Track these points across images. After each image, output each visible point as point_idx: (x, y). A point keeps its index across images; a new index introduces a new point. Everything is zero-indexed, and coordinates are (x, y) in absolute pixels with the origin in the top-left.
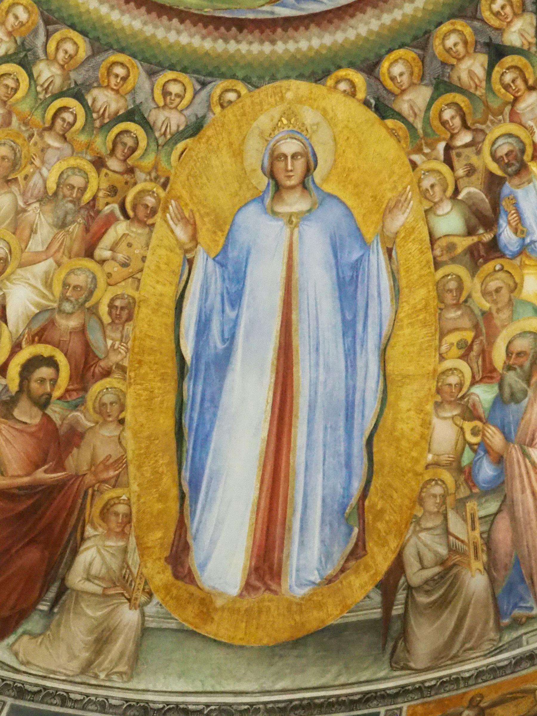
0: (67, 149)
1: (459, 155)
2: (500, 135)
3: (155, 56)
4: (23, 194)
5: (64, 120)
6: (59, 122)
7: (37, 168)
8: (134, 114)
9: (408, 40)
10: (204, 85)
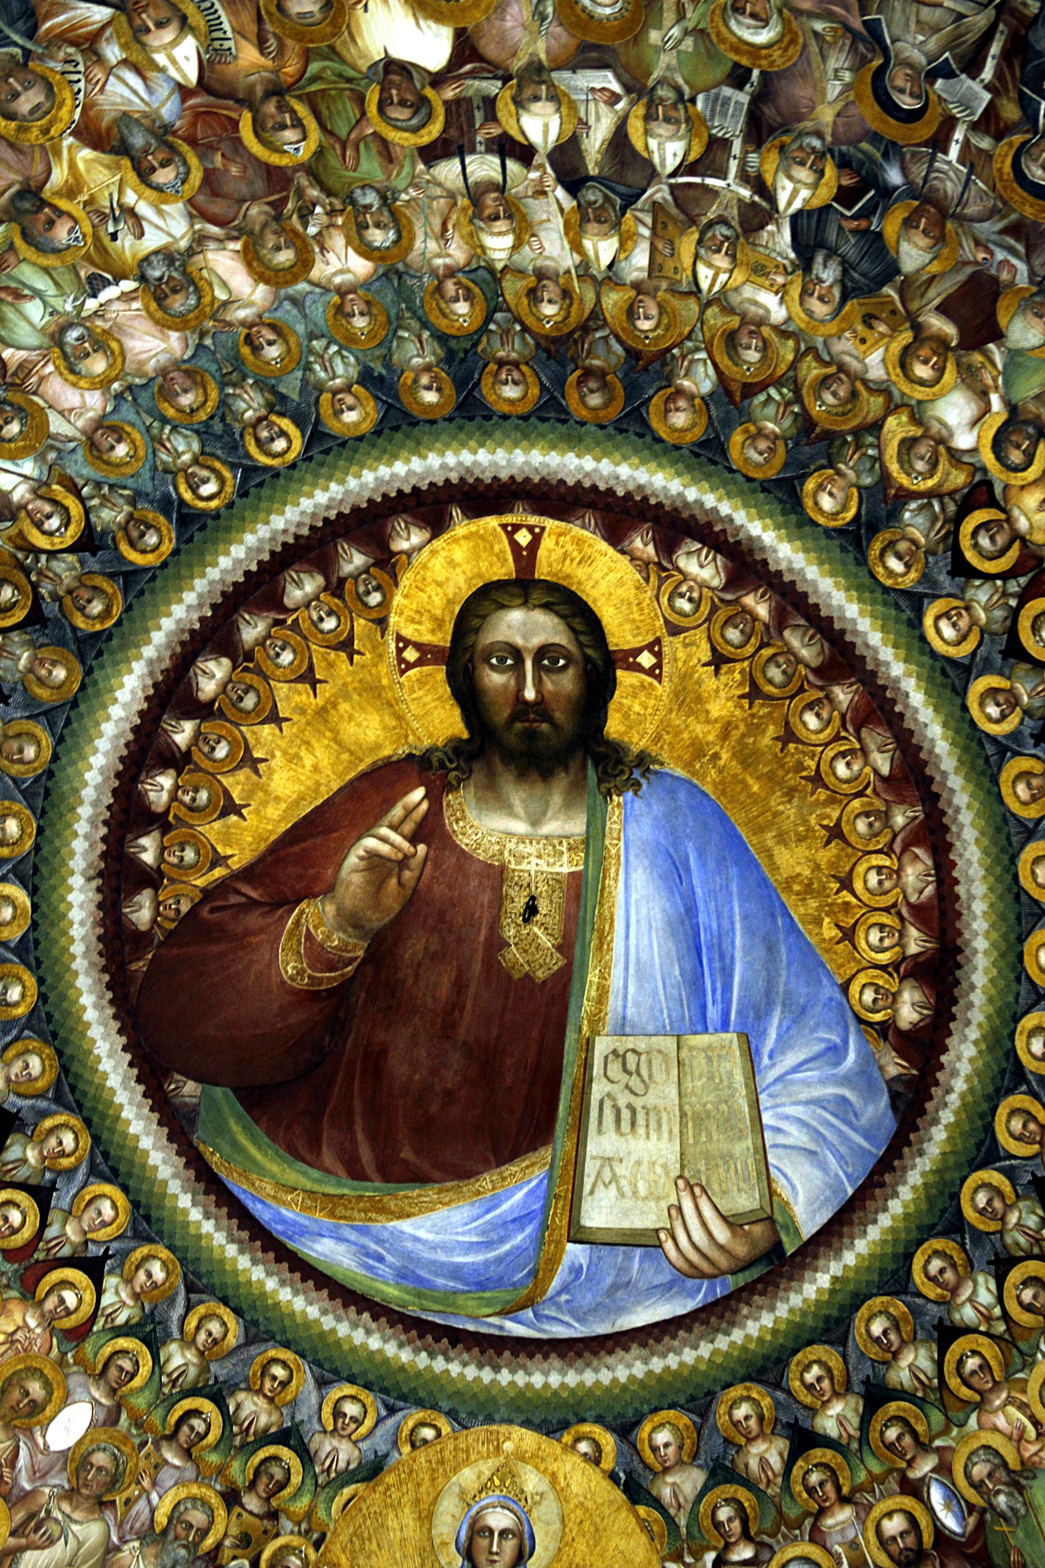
0: (190, 1473)
3: (330, 1359)
4: (120, 1526)
5: (192, 1428)
6: (185, 1429)
7: (144, 1490)
8: (289, 1436)
10: (392, 1410)
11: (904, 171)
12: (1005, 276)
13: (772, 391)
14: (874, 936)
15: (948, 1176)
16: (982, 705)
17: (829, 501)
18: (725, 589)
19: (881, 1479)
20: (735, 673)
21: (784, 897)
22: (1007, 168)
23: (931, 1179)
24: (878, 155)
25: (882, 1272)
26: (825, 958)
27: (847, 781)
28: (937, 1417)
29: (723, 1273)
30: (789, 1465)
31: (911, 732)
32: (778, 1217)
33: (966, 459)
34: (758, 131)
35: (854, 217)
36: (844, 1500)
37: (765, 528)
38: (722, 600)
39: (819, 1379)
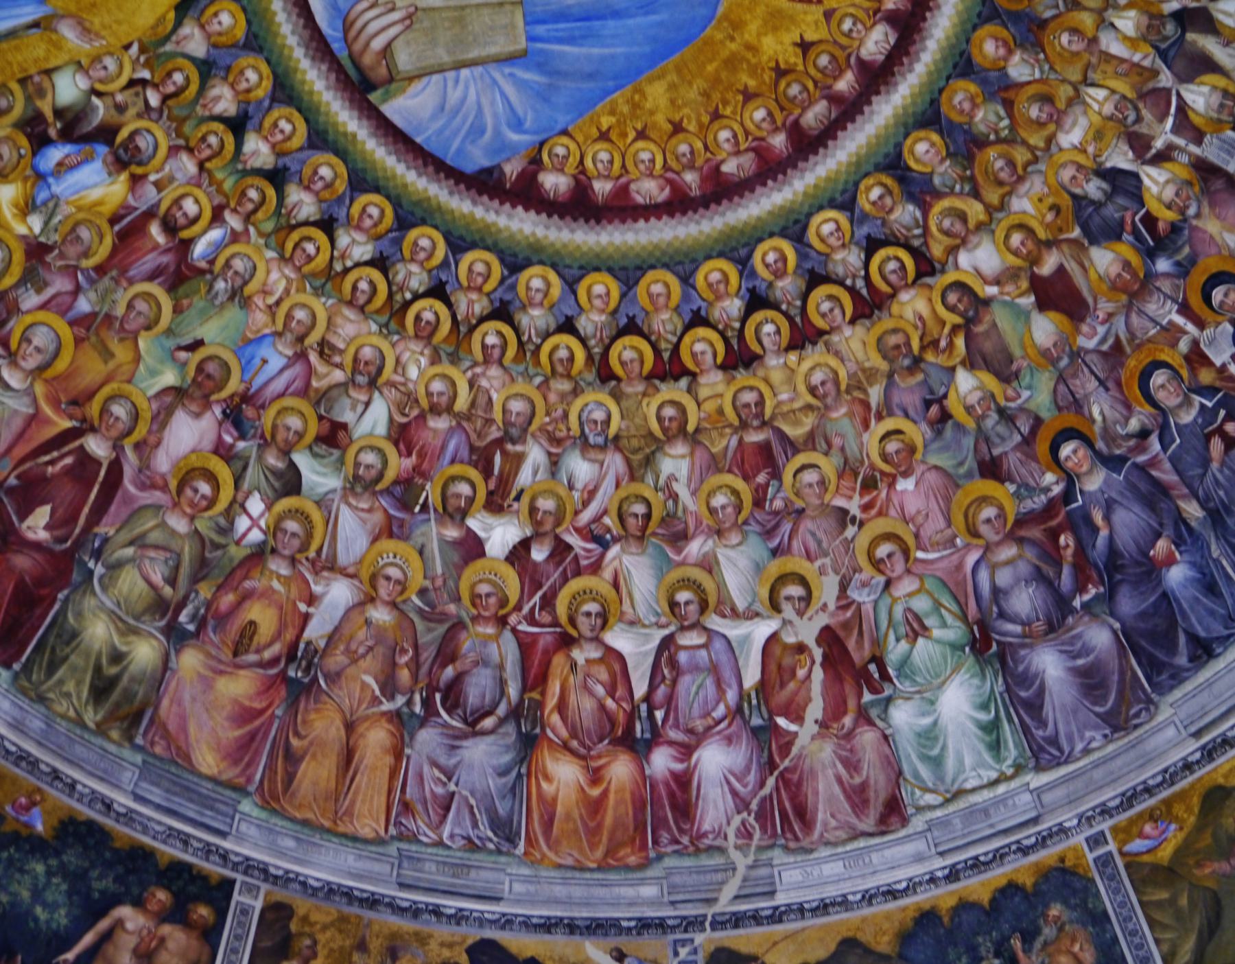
1: (137, 94)
2: (154, 137)
9: (254, 28)
11: (1166, 275)
12: (1085, 328)
13: (1006, 122)
14: (604, 156)
15: (437, 215)
16: (775, 249)
17: (924, 150)
18: (859, 59)
19: (220, 190)
20: (793, 57)
21: (629, 87)
22: (1163, 357)
23: (434, 202)
24: (1179, 257)
25: (364, 170)
26: (587, 117)
27: (715, 139)
28: (269, 226)
29: (349, 47)
30: (220, 119)
31: (752, 191)
32: (394, 86)
33: (951, 259)
34: (1205, 170)
35: (1133, 222)
36: (201, 166)
37: (904, 98)
38: (849, 55)
39: (282, 131)
